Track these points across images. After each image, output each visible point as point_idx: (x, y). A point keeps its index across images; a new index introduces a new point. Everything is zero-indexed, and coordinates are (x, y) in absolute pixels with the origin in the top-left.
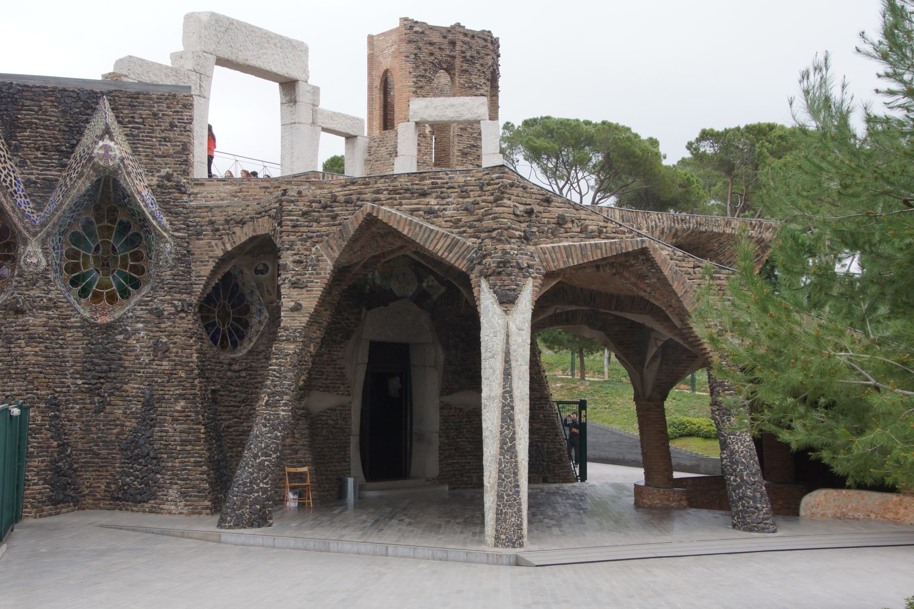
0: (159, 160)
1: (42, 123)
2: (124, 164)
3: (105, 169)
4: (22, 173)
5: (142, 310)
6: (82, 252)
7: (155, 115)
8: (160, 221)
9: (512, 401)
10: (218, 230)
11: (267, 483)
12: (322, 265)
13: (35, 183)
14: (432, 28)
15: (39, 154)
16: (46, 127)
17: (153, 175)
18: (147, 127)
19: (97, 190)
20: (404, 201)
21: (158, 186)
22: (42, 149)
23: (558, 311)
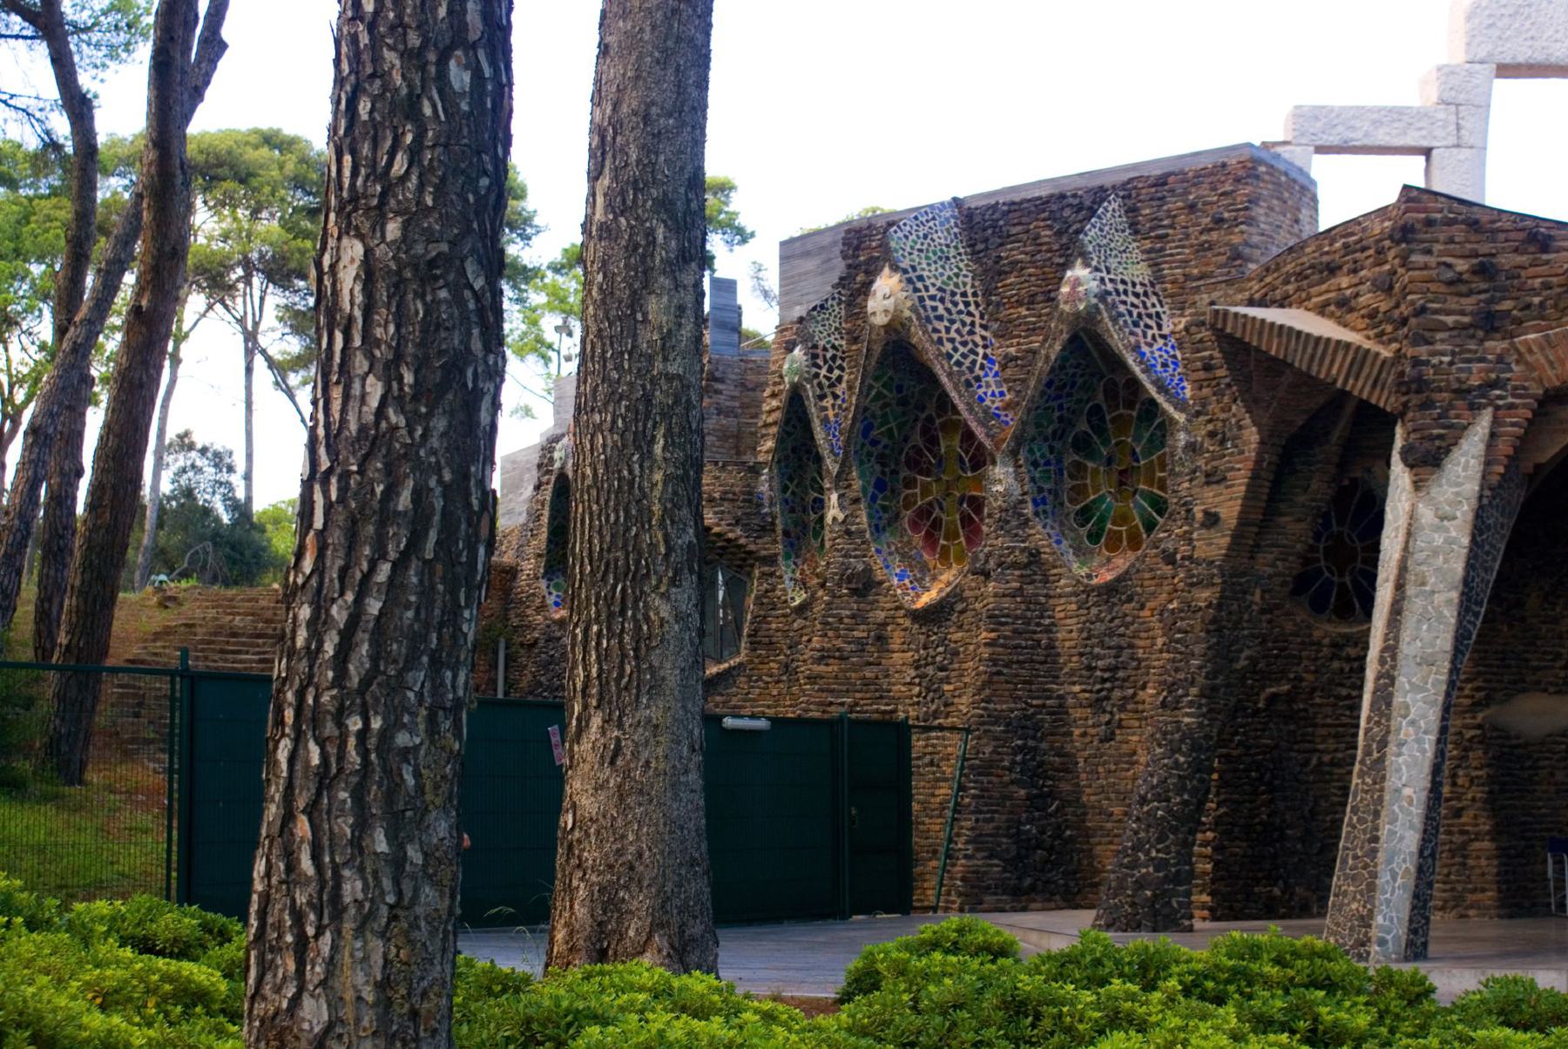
3: (1077, 315)
7: (1192, 207)
9: (1394, 667)
11: (1167, 851)
13: (1016, 358)
17: (1182, 315)
18: (1179, 230)
19: (1088, 354)
20: (1313, 290)
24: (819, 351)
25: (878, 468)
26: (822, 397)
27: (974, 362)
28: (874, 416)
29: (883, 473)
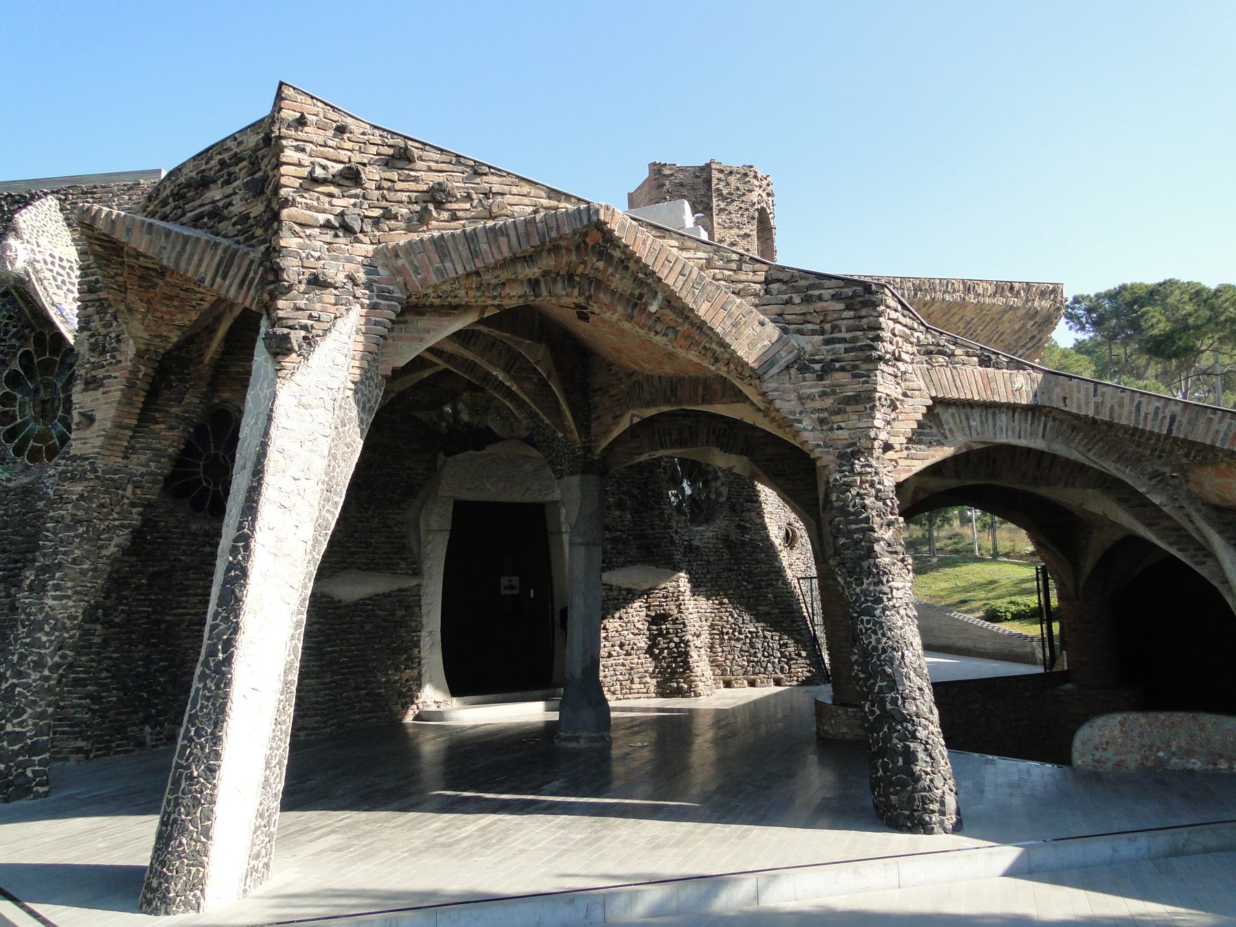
2: (34, 268)
6: (19, 396)
12: (123, 347)
14: (681, 169)
23: (636, 420)
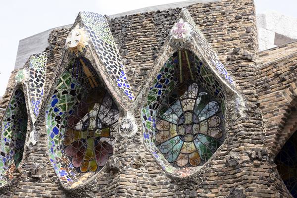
0: (227, 43)
1: (142, 34)
4: (127, 68)
5: (219, 163)
7: (224, 13)
8: (231, 83)
10: (284, 80)
15: (139, 54)
16: (145, 36)
19: (177, 67)
21: (228, 60)
22: (141, 49)
24: (34, 72)
25: (56, 123)
26: (33, 90)
27: (116, 70)
28: (59, 96)
29: (58, 126)
